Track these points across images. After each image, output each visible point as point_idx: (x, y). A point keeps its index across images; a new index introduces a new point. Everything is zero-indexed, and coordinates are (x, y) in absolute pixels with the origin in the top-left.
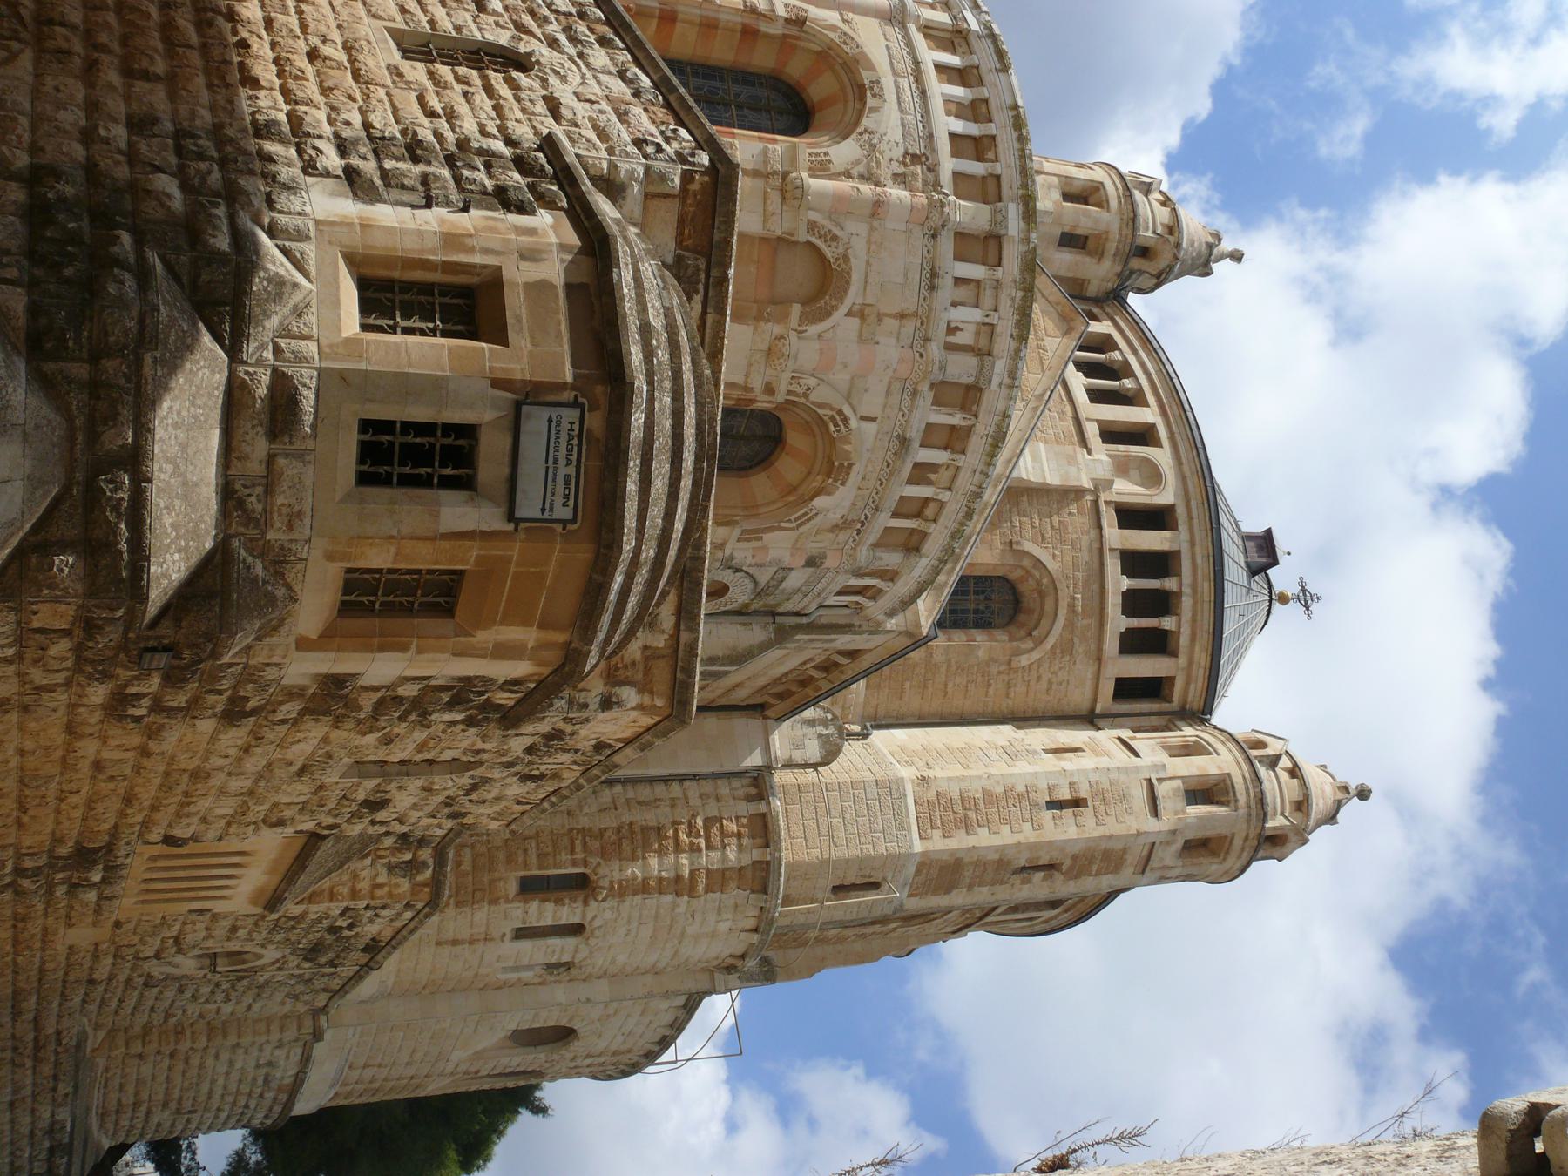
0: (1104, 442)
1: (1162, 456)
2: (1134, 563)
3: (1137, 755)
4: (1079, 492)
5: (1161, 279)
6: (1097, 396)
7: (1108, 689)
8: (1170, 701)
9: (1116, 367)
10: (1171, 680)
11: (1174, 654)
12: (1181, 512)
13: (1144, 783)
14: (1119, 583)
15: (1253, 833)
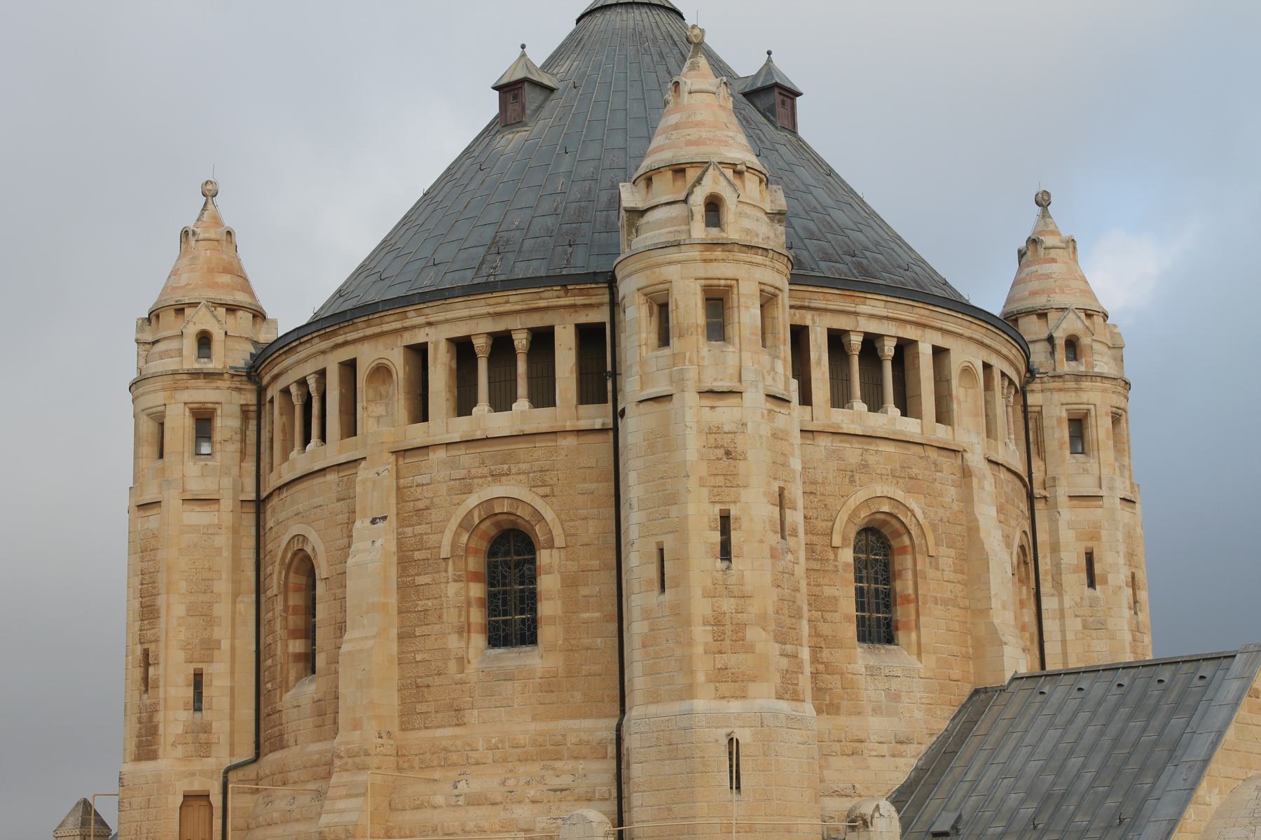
6: (323, 437)
8: (604, 324)
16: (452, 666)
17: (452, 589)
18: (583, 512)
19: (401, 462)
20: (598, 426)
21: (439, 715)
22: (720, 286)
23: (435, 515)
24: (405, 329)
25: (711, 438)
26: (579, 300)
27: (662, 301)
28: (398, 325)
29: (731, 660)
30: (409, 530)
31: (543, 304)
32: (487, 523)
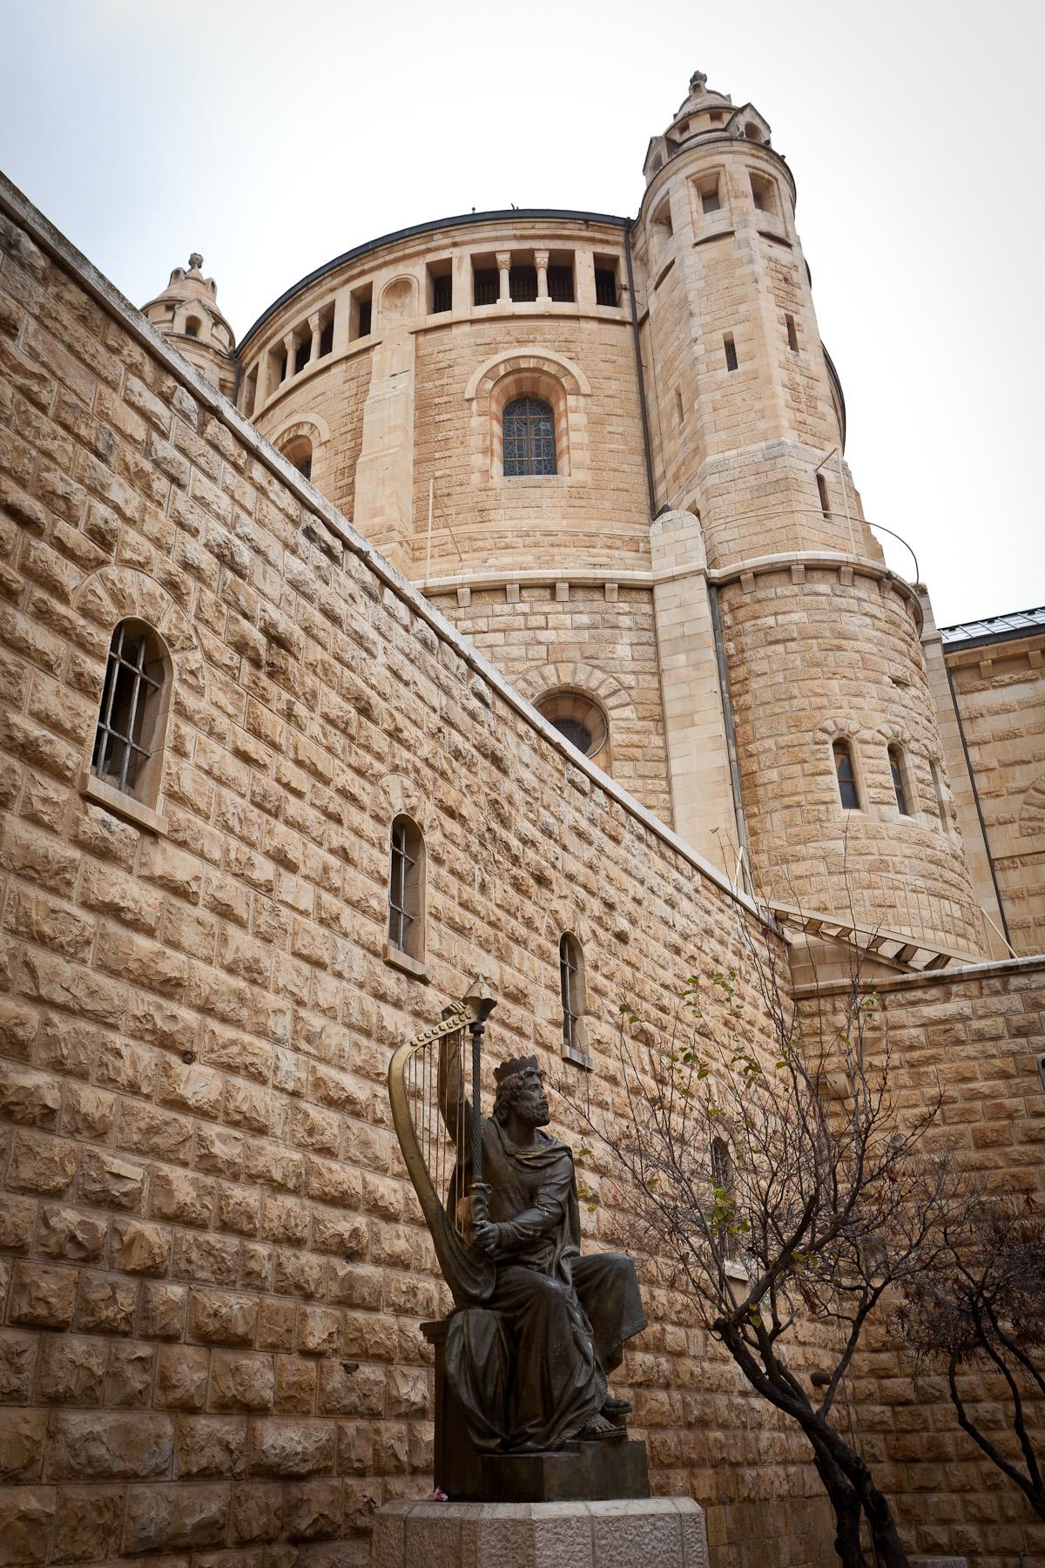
0: (369, 332)
1: (381, 280)
2: (485, 289)
3: (673, 263)
4: (417, 349)
5: (218, 320)
6: (326, 347)
7: (607, 312)
8: (615, 260)
9: (299, 341)
10: (598, 258)
11: (573, 251)
12: (431, 257)
13: (698, 248)
14: (505, 304)
15: (745, 147)
16: (476, 478)
17: (476, 422)
18: (606, 374)
19: (421, 339)
20: (618, 318)
21: (461, 516)
22: (763, 178)
23: (457, 370)
24: (429, 250)
25: (772, 265)
26: (598, 236)
27: (709, 187)
28: (423, 247)
29: (810, 420)
30: (430, 385)
31: (565, 232)
32: (510, 379)
